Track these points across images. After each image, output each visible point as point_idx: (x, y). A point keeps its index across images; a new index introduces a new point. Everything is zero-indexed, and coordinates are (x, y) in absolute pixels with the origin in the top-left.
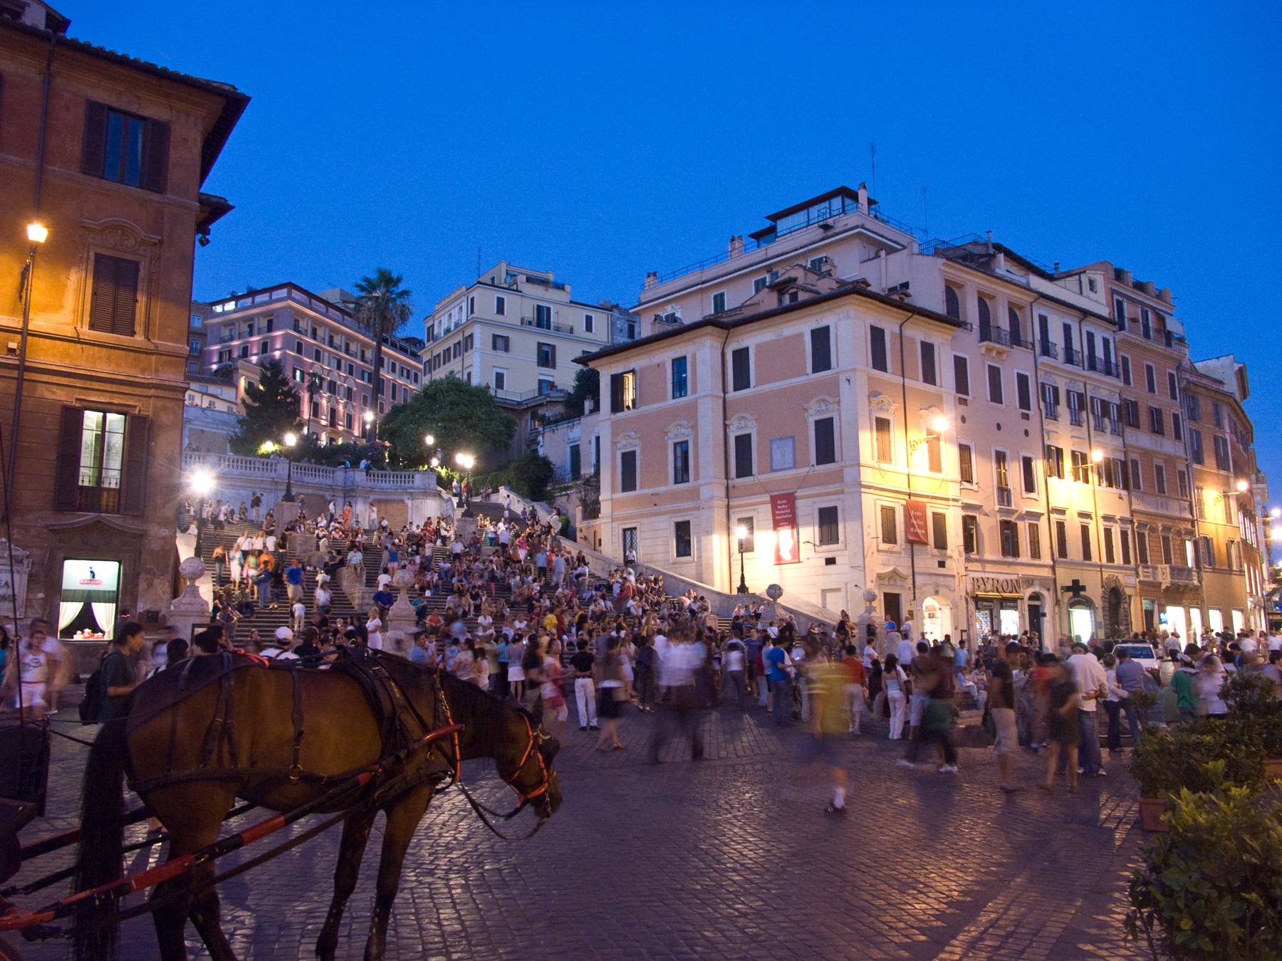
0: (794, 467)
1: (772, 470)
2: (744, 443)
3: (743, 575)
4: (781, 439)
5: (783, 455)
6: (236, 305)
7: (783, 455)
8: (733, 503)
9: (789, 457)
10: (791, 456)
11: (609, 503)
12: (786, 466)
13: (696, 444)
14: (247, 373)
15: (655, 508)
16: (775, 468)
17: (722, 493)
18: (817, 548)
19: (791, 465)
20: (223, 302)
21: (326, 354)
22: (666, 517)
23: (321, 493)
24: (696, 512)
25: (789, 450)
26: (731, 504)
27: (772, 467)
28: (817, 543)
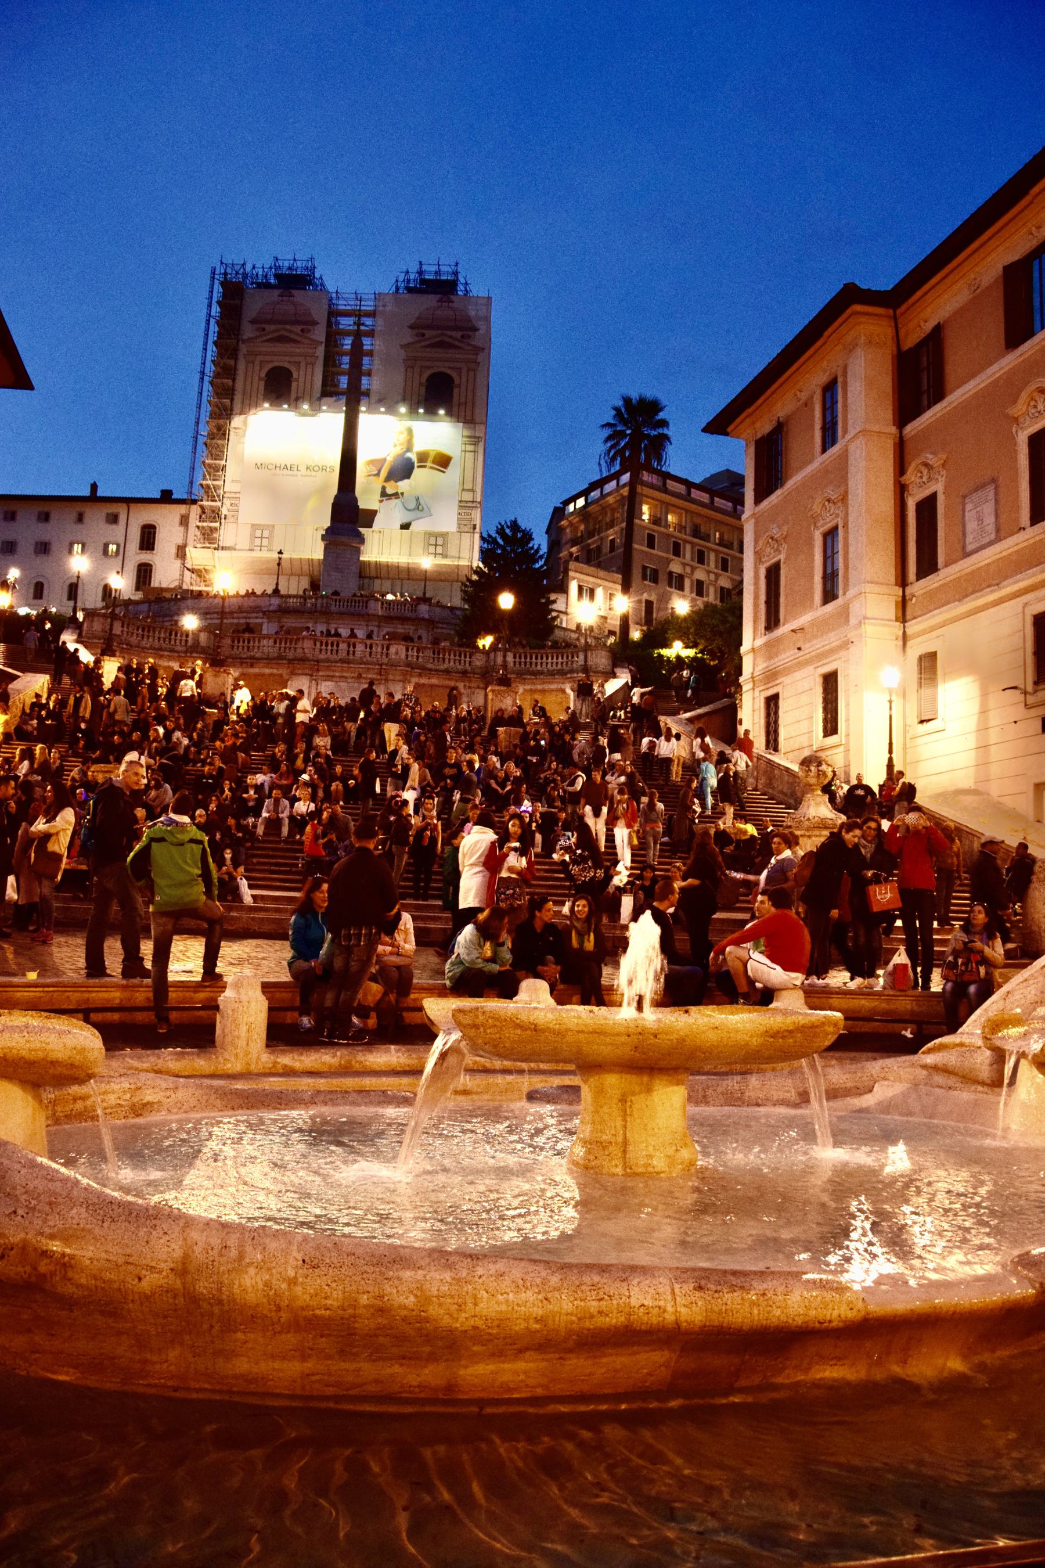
0: (998, 539)
1: (967, 555)
2: (928, 507)
3: (890, 760)
4: (976, 490)
5: (980, 520)
6: (586, 500)
7: (980, 520)
8: (912, 627)
9: (990, 520)
10: (992, 519)
11: (751, 655)
12: (987, 540)
13: (846, 526)
14: (607, 584)
15: (801, 653)
16: (970, 548)
17: (890, 610)
18: (1031, 700)
19: (993, 537)
20: (574, 499)
21: (712, 556)
22: (811, 668)
23: (452, 684)
24: (842, 653)
25: (988, 509)
26: (909, 631)
27: (964, 547)
28: (1030, 688)
